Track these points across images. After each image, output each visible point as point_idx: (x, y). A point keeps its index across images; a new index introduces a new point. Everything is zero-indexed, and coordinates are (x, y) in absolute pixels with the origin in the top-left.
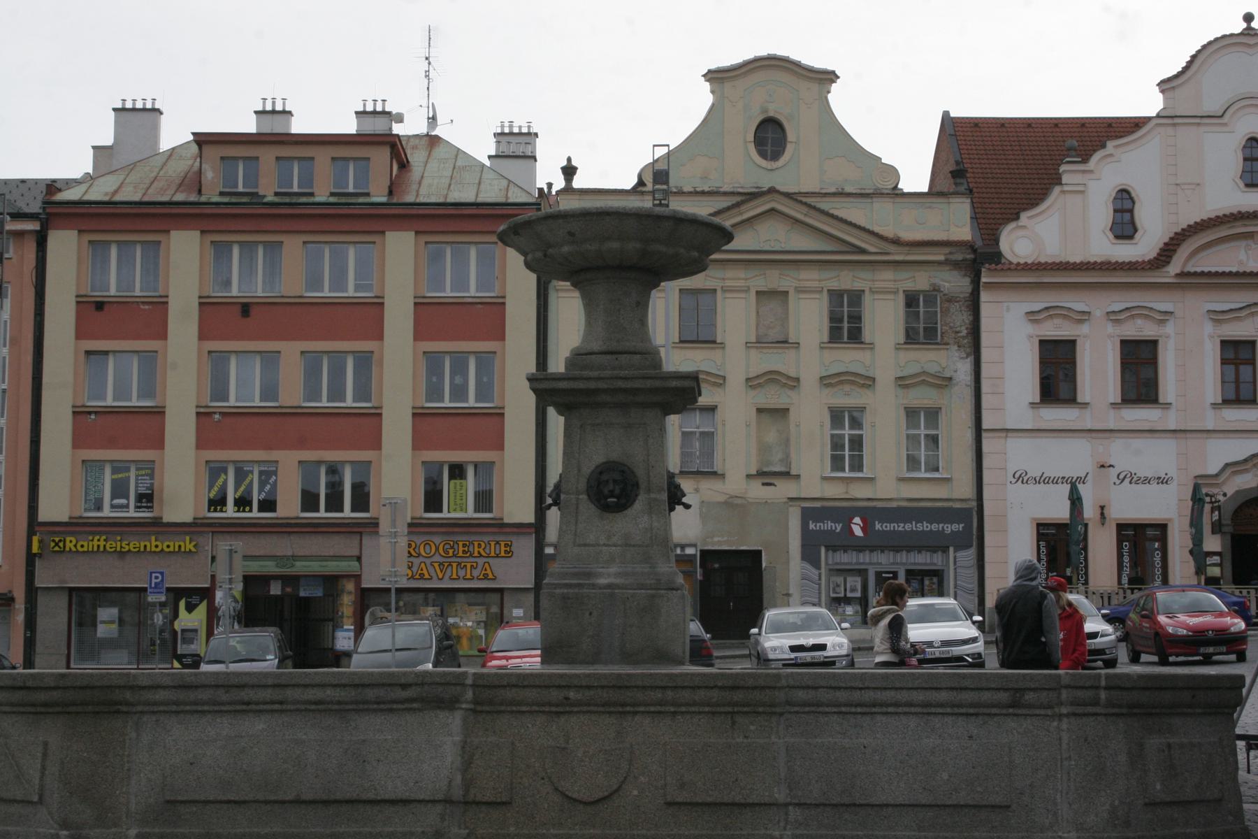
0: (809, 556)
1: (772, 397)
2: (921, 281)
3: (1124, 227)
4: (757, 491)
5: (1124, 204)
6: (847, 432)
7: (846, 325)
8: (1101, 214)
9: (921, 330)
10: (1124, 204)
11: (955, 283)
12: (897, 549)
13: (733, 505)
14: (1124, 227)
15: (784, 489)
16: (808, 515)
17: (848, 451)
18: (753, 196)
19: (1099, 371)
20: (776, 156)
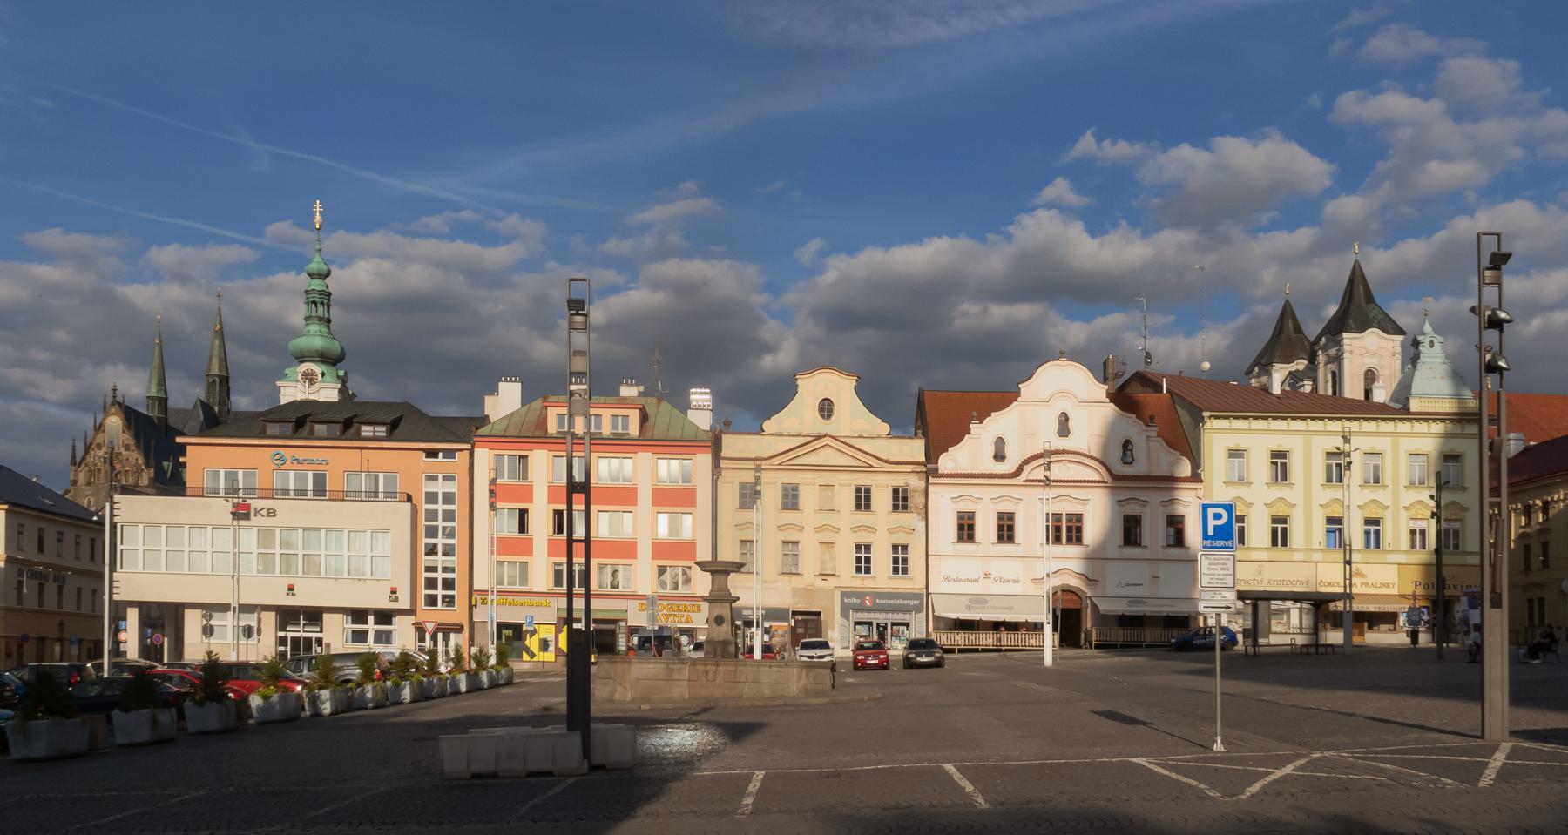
0: (845, 615)
1: (827, 537)
2: (899, 481)
3: (999, 457)
4: (819, 583)
5: (1000, 442)
6: (863, 555)
7: (863, 500)
8: (990, 450)
9: (900, 500)
10: (1000, 442)
11: (916, 483)
12: (887, 611)
13: (808, 592)
14: (999, 457)
15: (832, 582)
16: (844, 595)
17: (863, 565)
18: (819, 437)
19: (986, 528)
20: (829, 417)
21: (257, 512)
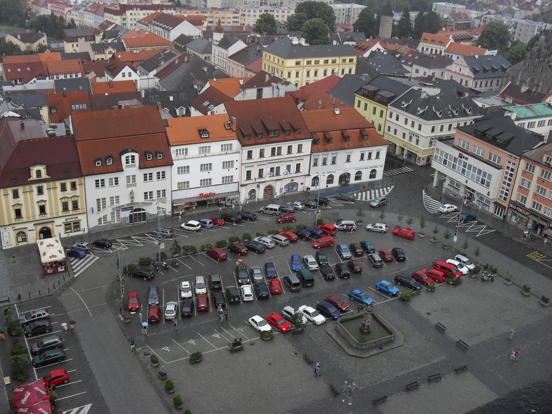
21: (464, 157)
